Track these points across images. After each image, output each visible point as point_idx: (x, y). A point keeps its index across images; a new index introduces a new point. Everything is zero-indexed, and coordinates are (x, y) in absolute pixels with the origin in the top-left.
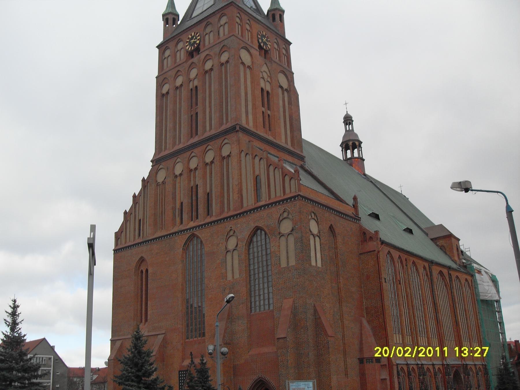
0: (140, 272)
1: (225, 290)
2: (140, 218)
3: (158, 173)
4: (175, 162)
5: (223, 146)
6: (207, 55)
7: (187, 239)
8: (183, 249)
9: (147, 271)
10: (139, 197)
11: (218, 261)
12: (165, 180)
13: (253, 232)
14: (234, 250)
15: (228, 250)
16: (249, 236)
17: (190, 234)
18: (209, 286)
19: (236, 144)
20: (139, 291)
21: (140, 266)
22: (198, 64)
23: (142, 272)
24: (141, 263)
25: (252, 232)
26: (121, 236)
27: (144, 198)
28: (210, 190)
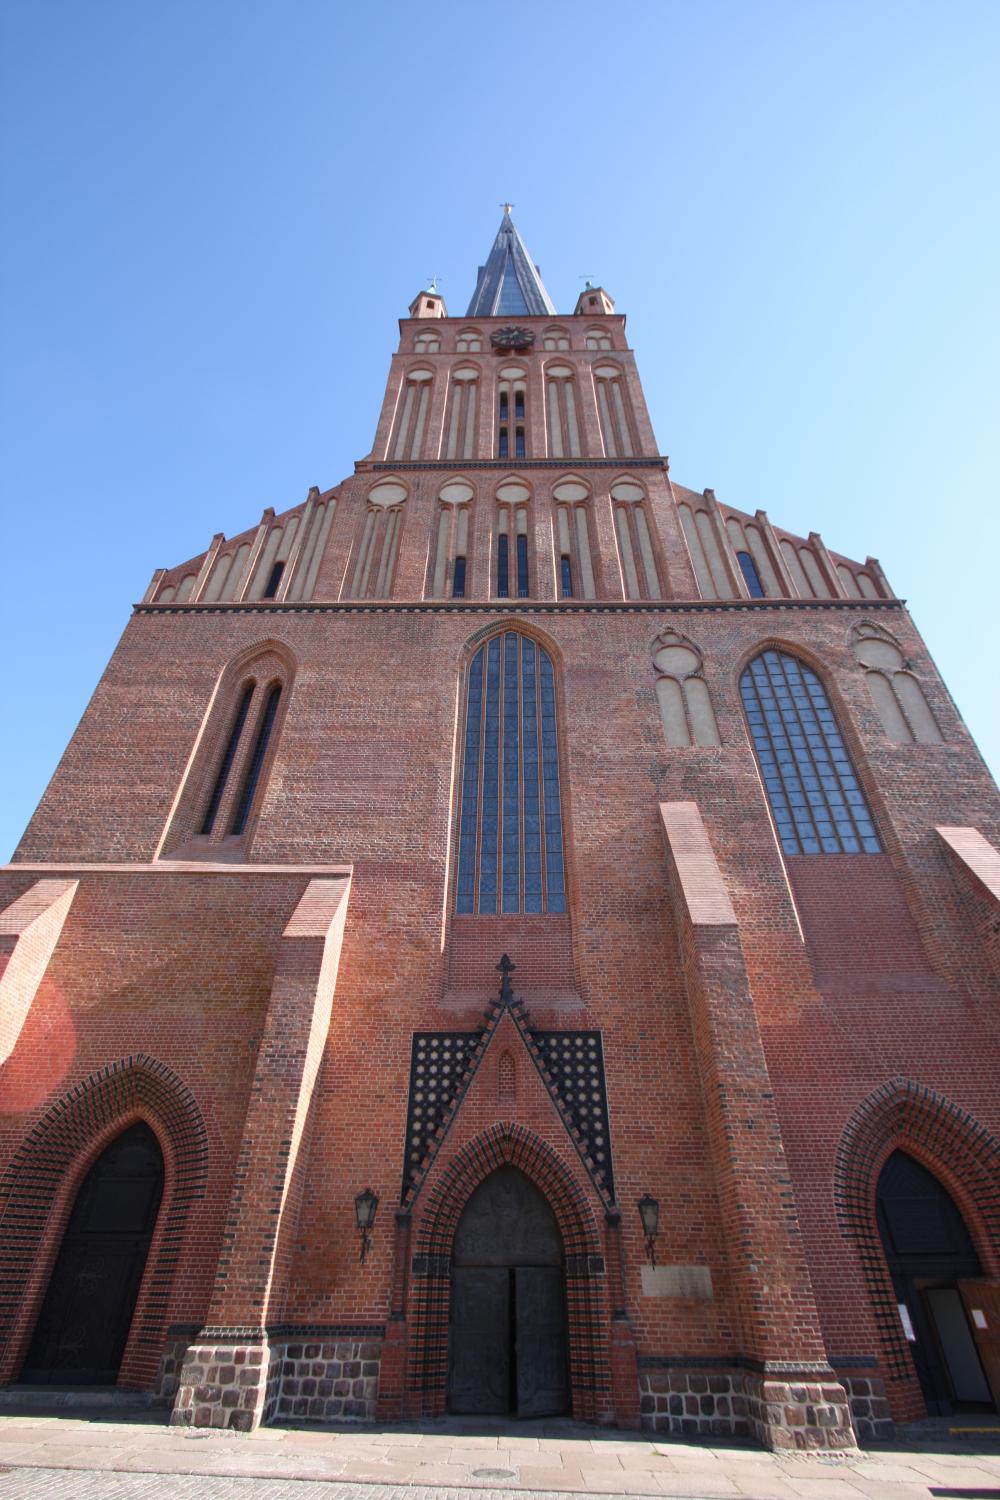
0: (239, 683)
1: (663, 772)
2: (279, 558)
4: (446, 481)
5: (617, 485)
7: (487, 628)
8: (465, 647)
9: (275, 691)
10: (290, 519)
11: (624, 696)
12: (404, 504)
13: (756, 650)
14: (689, 677)
15: (666, 674)
16: (744, 655)
17: (498, 619)
18: (588, 753)
20: (223, 734)
21: (247, 664)
23: (249, 688)
24: (256, 659)
25: (753, 648)
26: (181, 582)
27: (311, 521)
28: (572, 545)
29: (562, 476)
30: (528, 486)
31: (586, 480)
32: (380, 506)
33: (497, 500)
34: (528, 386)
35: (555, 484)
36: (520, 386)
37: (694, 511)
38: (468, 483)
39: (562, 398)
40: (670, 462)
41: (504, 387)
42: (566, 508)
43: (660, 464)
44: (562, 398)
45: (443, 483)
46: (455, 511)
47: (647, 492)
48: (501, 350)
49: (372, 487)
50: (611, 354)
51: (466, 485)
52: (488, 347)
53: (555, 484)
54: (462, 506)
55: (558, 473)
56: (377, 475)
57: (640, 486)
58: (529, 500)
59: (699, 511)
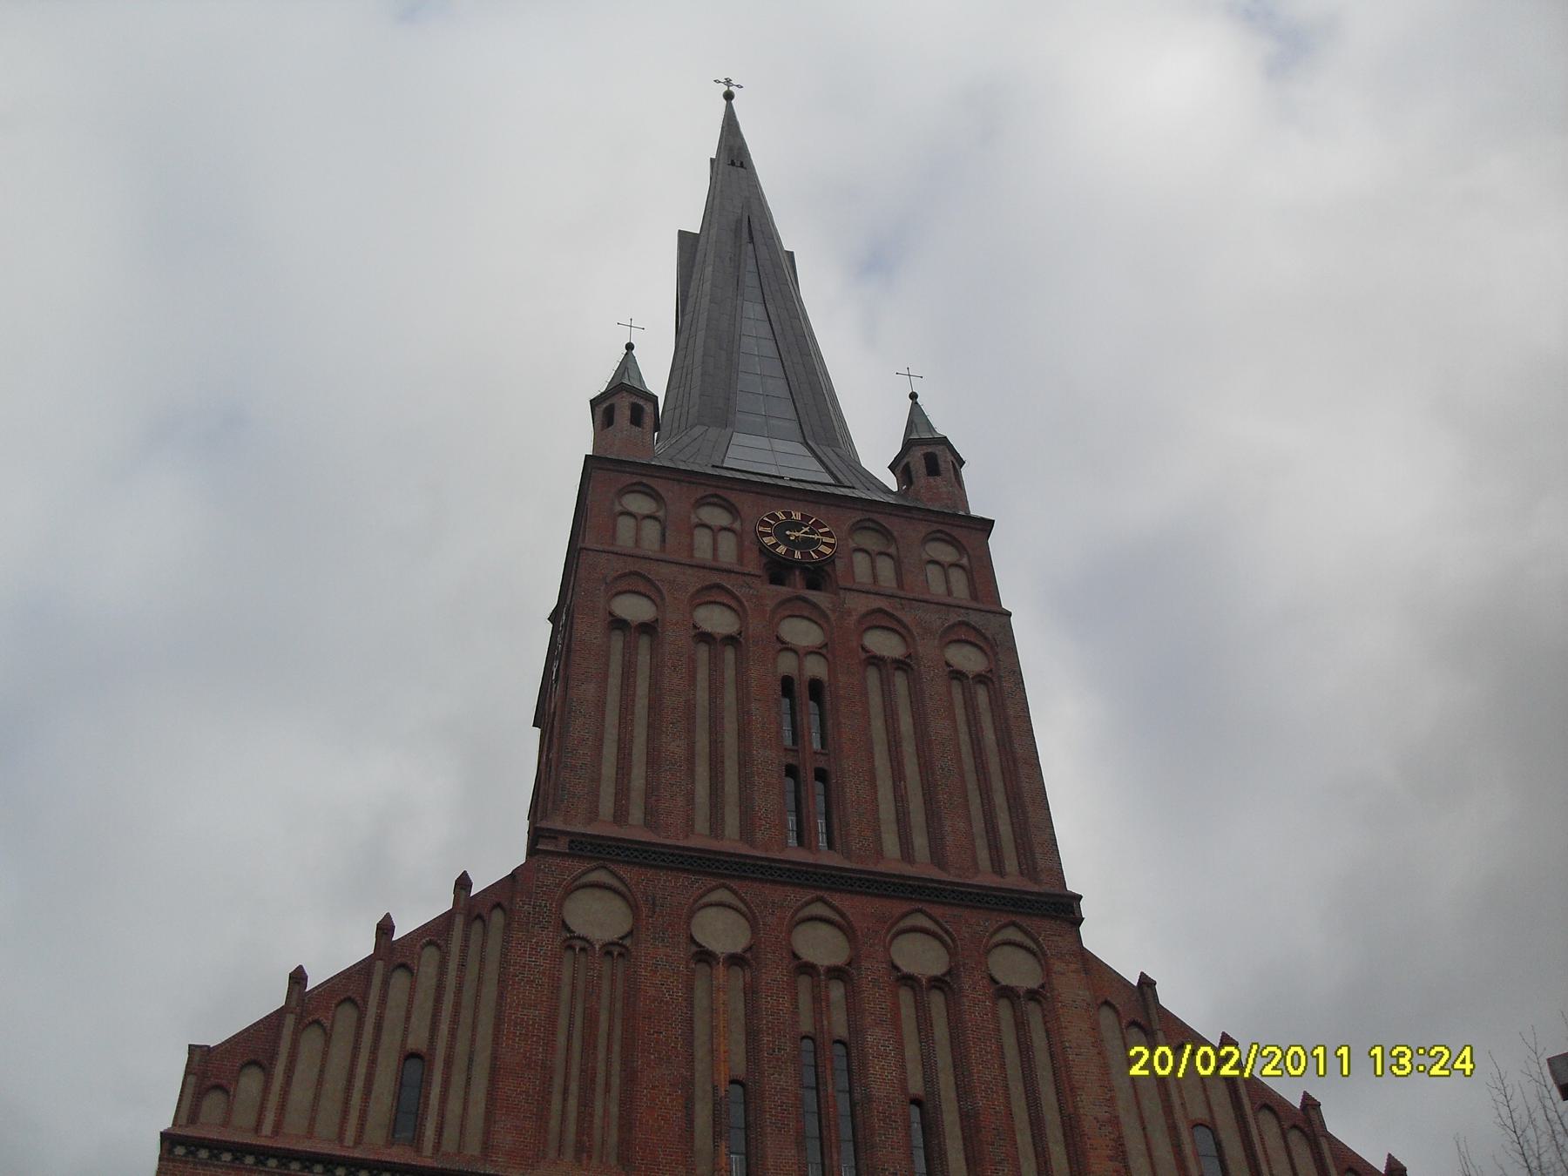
3: (573, 896)
4: (701, 897)
6: (880, 610)
10: (422, 948)
19: (1073, 967)
22: (833, 617)
29: (904, 916)
30: (845, 928)
31: (946, 931)
32: (588, 941)
33: (795, 956)
34: (831, 671)
35: (894, 930)
36: (816, 668)
37: (1124, 1023)
38: (741, 906)
39: (1021, 1025)
40: (1084, 906)
41: (787, 664)
42: (913, 988)
43: (1067, 909)
44: (1021, 1025)
45: (696, 901)
46: (720, 970)
47: (1047, 971)
48: (778, 570)
49: (570, 891)
50: (974, 618)
51: (736, 909)
52: (753, 564)
53: (894, 930)
54: (735, 960)
55: (898, 907)
56: (578, 866)
57: (1034, 954)
58: (849, 964)
59: (1134, 1023)
